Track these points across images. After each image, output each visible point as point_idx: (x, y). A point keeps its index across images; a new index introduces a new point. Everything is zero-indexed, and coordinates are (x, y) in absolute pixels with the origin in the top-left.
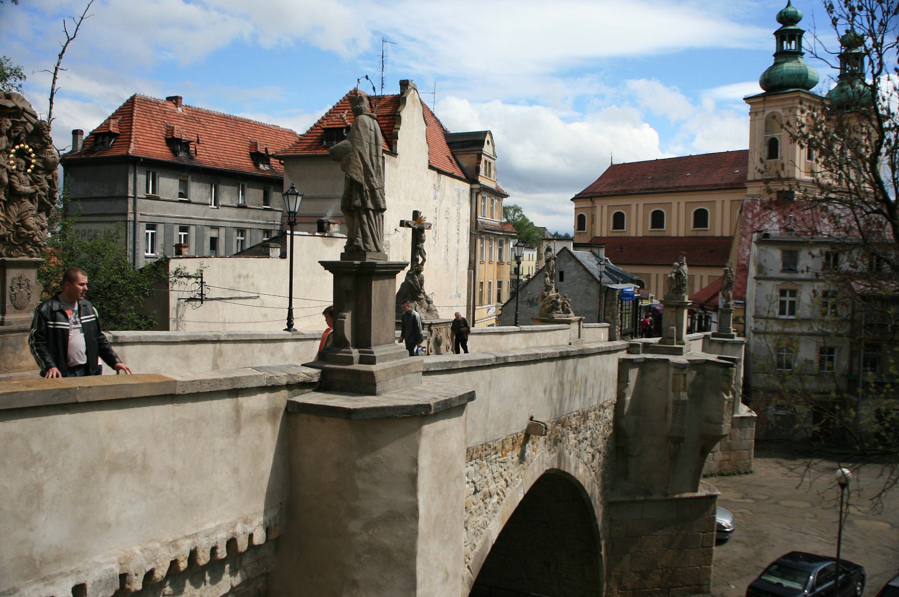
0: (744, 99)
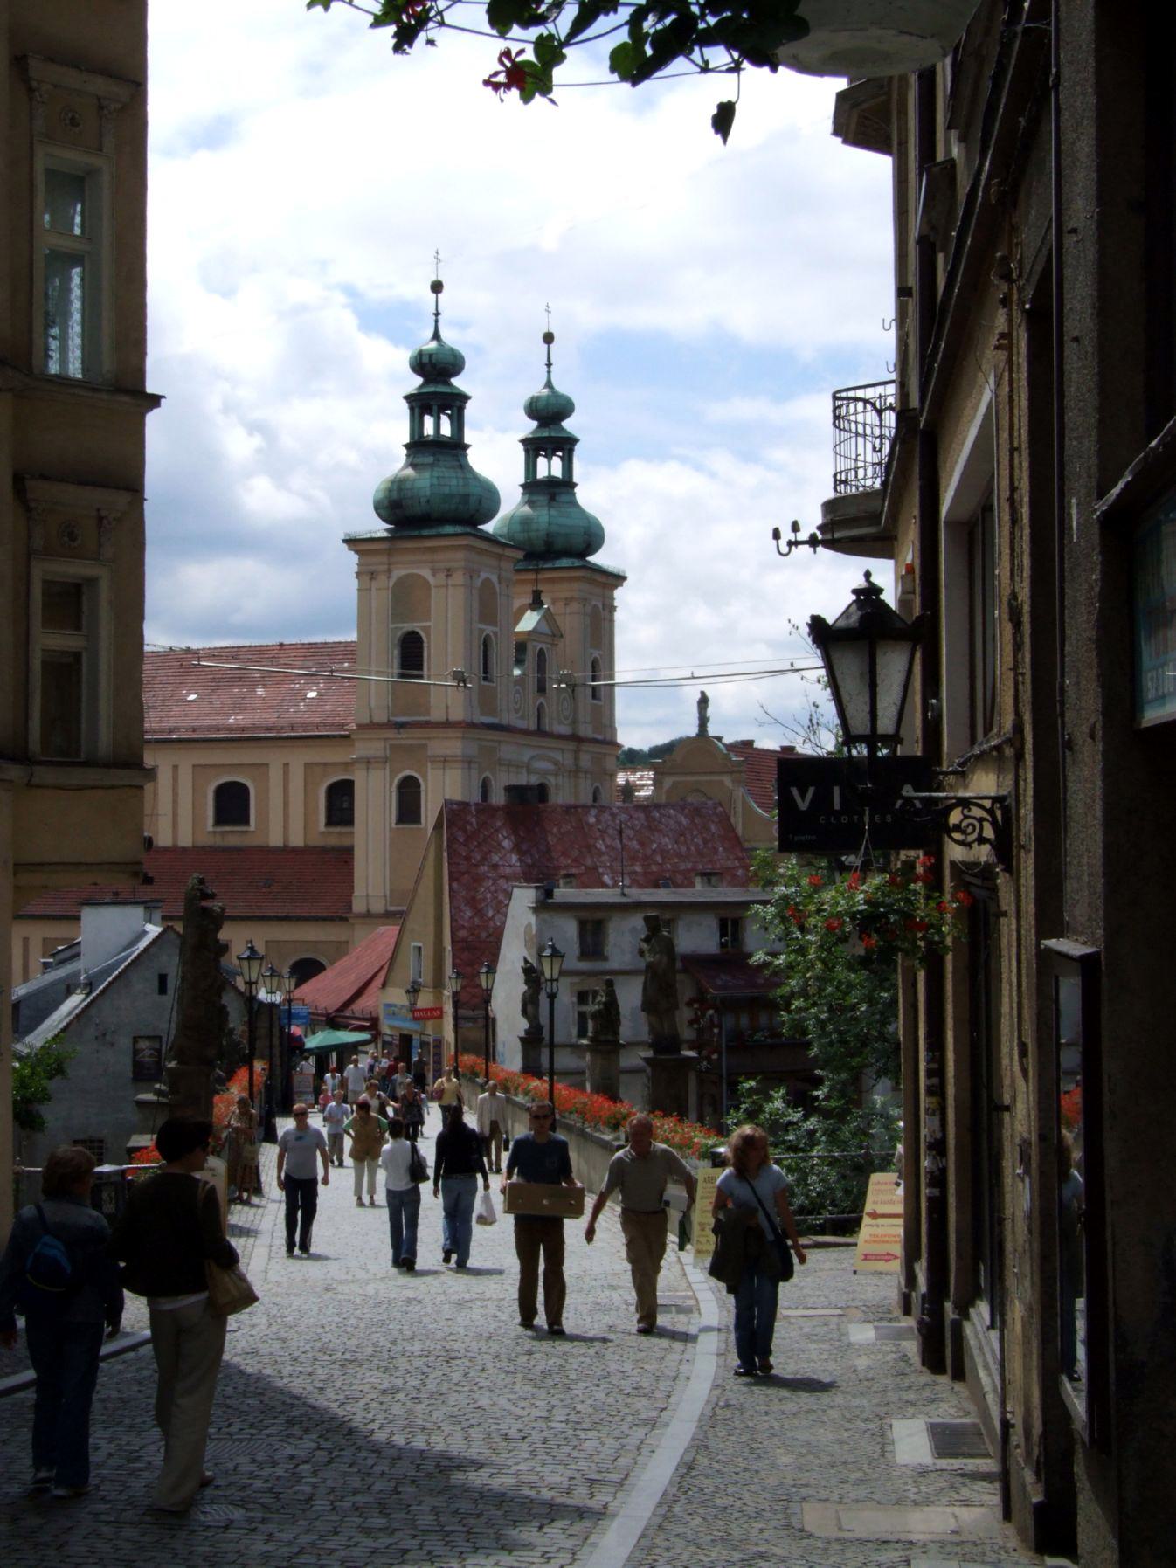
0: (345, 541)
